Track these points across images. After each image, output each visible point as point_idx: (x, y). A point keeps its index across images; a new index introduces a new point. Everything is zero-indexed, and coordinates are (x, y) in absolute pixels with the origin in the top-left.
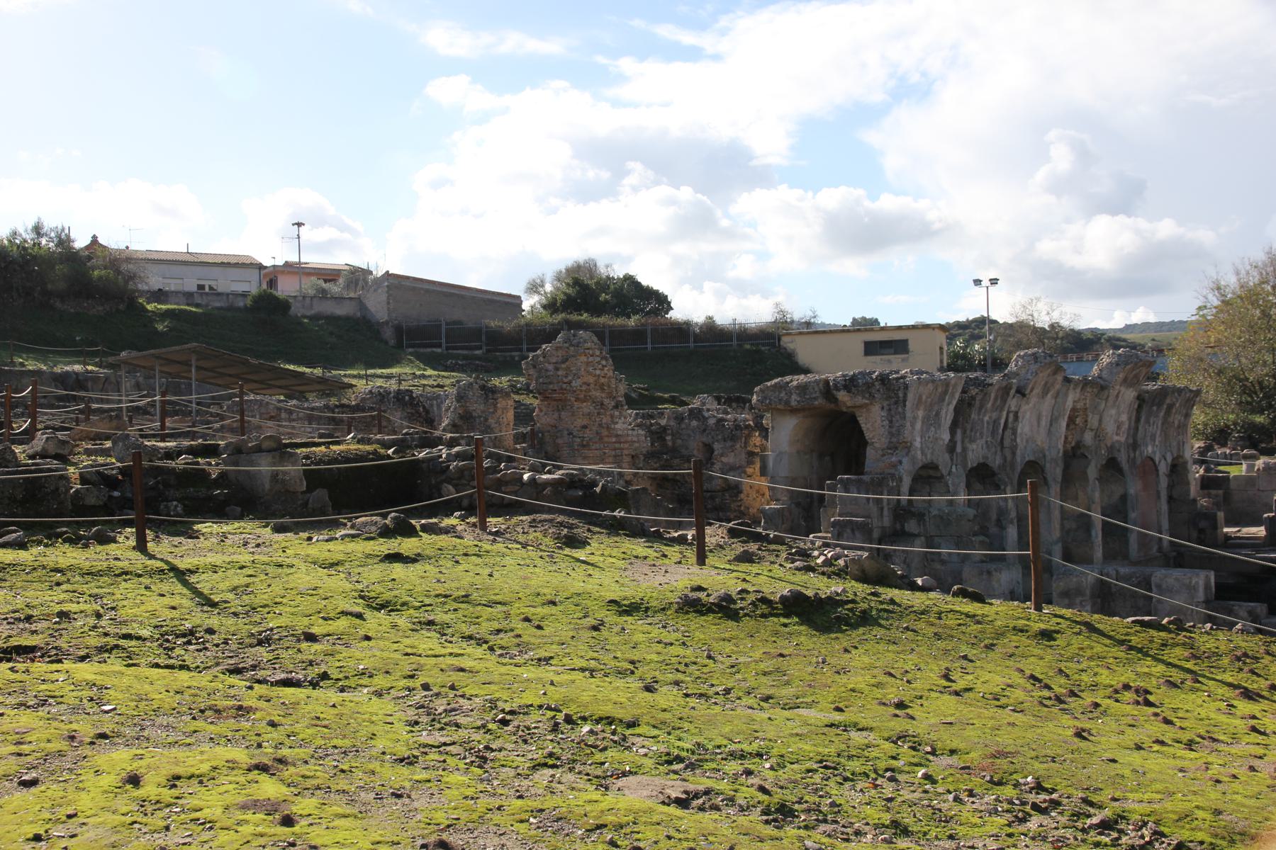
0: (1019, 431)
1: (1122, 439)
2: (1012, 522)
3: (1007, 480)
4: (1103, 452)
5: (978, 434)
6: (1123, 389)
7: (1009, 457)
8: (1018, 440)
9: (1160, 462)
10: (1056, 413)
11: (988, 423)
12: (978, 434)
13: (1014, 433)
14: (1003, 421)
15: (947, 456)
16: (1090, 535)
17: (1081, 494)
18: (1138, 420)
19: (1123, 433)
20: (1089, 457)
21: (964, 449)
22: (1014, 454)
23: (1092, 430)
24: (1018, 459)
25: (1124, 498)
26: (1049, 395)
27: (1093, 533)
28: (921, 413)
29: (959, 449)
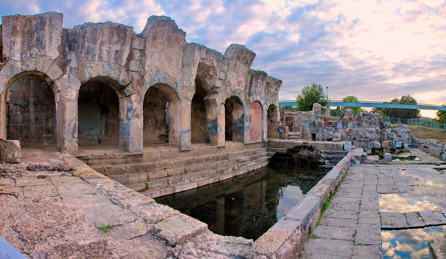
0: (147, 63)
1: (242, 89)
2: (137, 116)
3: (132, 90)
4: (228, 92)
5: (97, 57)
7: (136, 77)
8: (146, 69)
11: (109, 52)
12: (97, 57)
13: (142, 63)
16: (217, 131)
17: (214, 110)
18: (251, 83)
19: (242, 86)
20: (219, 92)
23: (221, 80)
24: (147, 79)
25: (243, 116)
27: (219, 129)
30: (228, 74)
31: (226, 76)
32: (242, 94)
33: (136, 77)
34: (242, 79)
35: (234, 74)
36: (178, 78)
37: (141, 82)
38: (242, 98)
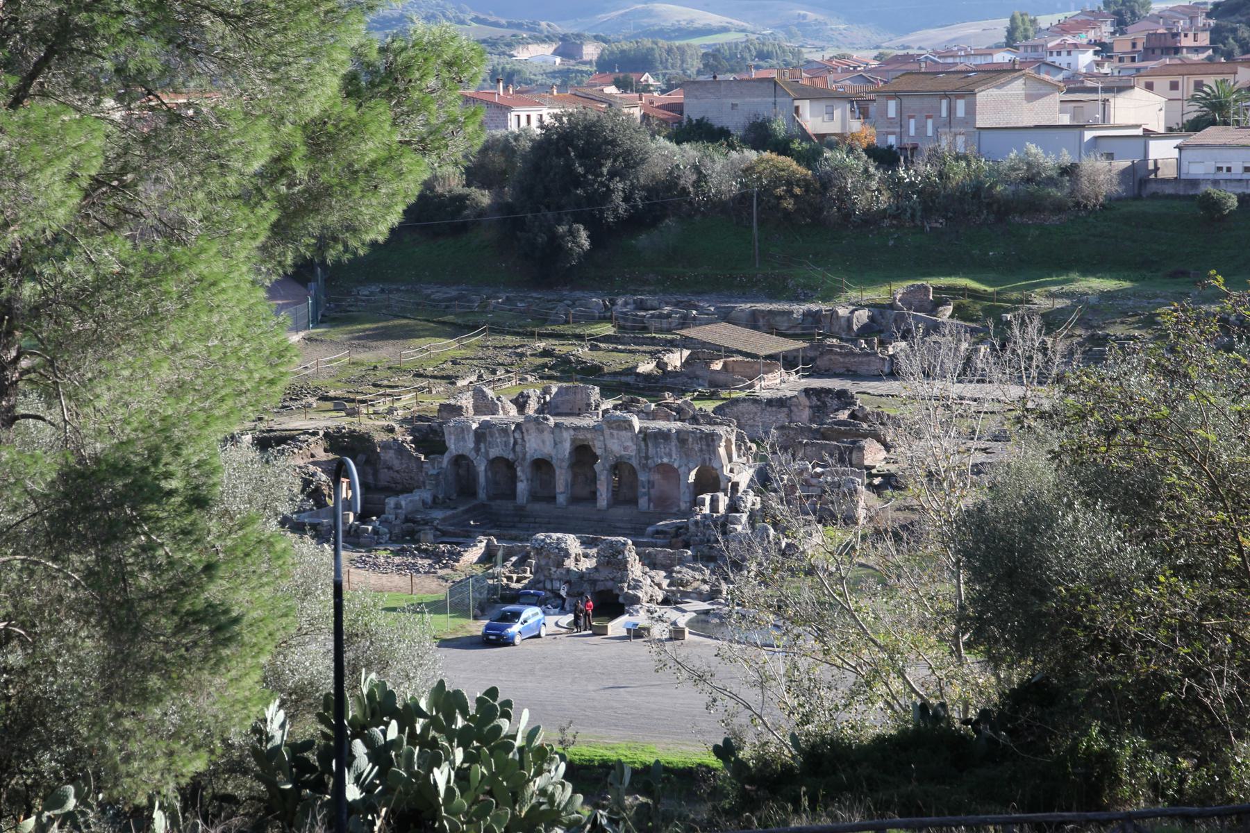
0: (527, 445)
1: (633, 454)
6: (615, 432)
7: (521, 456)
9: (680, 467)
10: (557, 440)
13: (524, 446)
14: (512, 441)
15: (473, 452)
18: (647, 445)
21: (487, 452)
22: (525, 454)
24: (528, 456)
26: (545, 433)
27: (598, 494)
28: (453, 437)
29: (483, 450)
30: (607, 442)
31: (605, 445)
32: (633, 459)
33: (521, 456)
34: (629, 444)
35: (615, 441)
36: (553, 453)
37: (524, 459)
38: (634, 463)
